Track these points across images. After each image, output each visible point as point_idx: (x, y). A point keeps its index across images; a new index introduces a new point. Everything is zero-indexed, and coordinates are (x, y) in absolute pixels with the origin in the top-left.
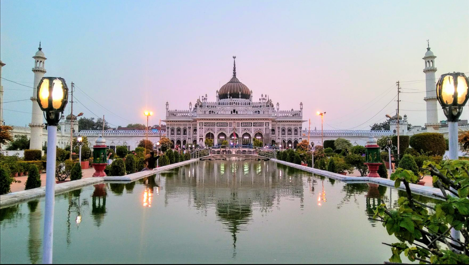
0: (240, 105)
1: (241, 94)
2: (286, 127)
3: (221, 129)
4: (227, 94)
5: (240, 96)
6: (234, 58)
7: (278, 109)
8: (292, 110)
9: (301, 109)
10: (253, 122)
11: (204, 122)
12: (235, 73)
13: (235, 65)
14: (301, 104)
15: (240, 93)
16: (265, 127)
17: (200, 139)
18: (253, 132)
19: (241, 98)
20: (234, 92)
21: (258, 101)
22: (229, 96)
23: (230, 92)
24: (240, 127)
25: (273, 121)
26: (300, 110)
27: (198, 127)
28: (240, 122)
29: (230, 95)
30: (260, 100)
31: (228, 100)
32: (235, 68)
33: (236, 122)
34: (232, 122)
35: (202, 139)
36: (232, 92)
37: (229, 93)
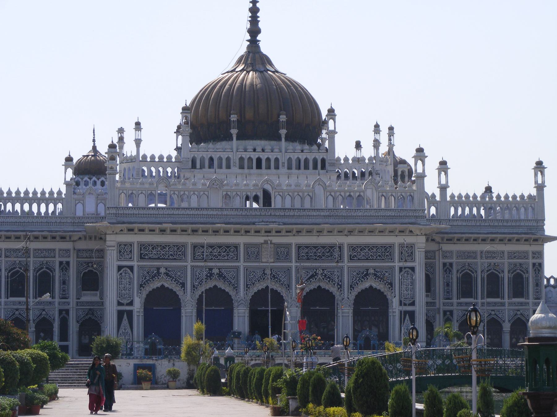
0: (283, 170)
1: (289, 124)
2: (481, 265)
3: (210, 275)
4: (228, 124)
5: (283, 132)
7: (443, 188)
8: (489, 190)
9: (540, 188)
11: (135, 239)
14: (539, 166)
15: (283, 118)
17: (120, 314)
19: (289, 138)
20: (256, 113)
21: (352, 153)
22: (234, 132)
23: (241, 114)
25: (430, 239)
26: (534, 192)
27: (112, 261)
29: (240, 124)
30: (358, 145)
31: (233, 149)
34: (259, 240)
35: (130, 314)
36: (249, 114)
37: (234, 118)
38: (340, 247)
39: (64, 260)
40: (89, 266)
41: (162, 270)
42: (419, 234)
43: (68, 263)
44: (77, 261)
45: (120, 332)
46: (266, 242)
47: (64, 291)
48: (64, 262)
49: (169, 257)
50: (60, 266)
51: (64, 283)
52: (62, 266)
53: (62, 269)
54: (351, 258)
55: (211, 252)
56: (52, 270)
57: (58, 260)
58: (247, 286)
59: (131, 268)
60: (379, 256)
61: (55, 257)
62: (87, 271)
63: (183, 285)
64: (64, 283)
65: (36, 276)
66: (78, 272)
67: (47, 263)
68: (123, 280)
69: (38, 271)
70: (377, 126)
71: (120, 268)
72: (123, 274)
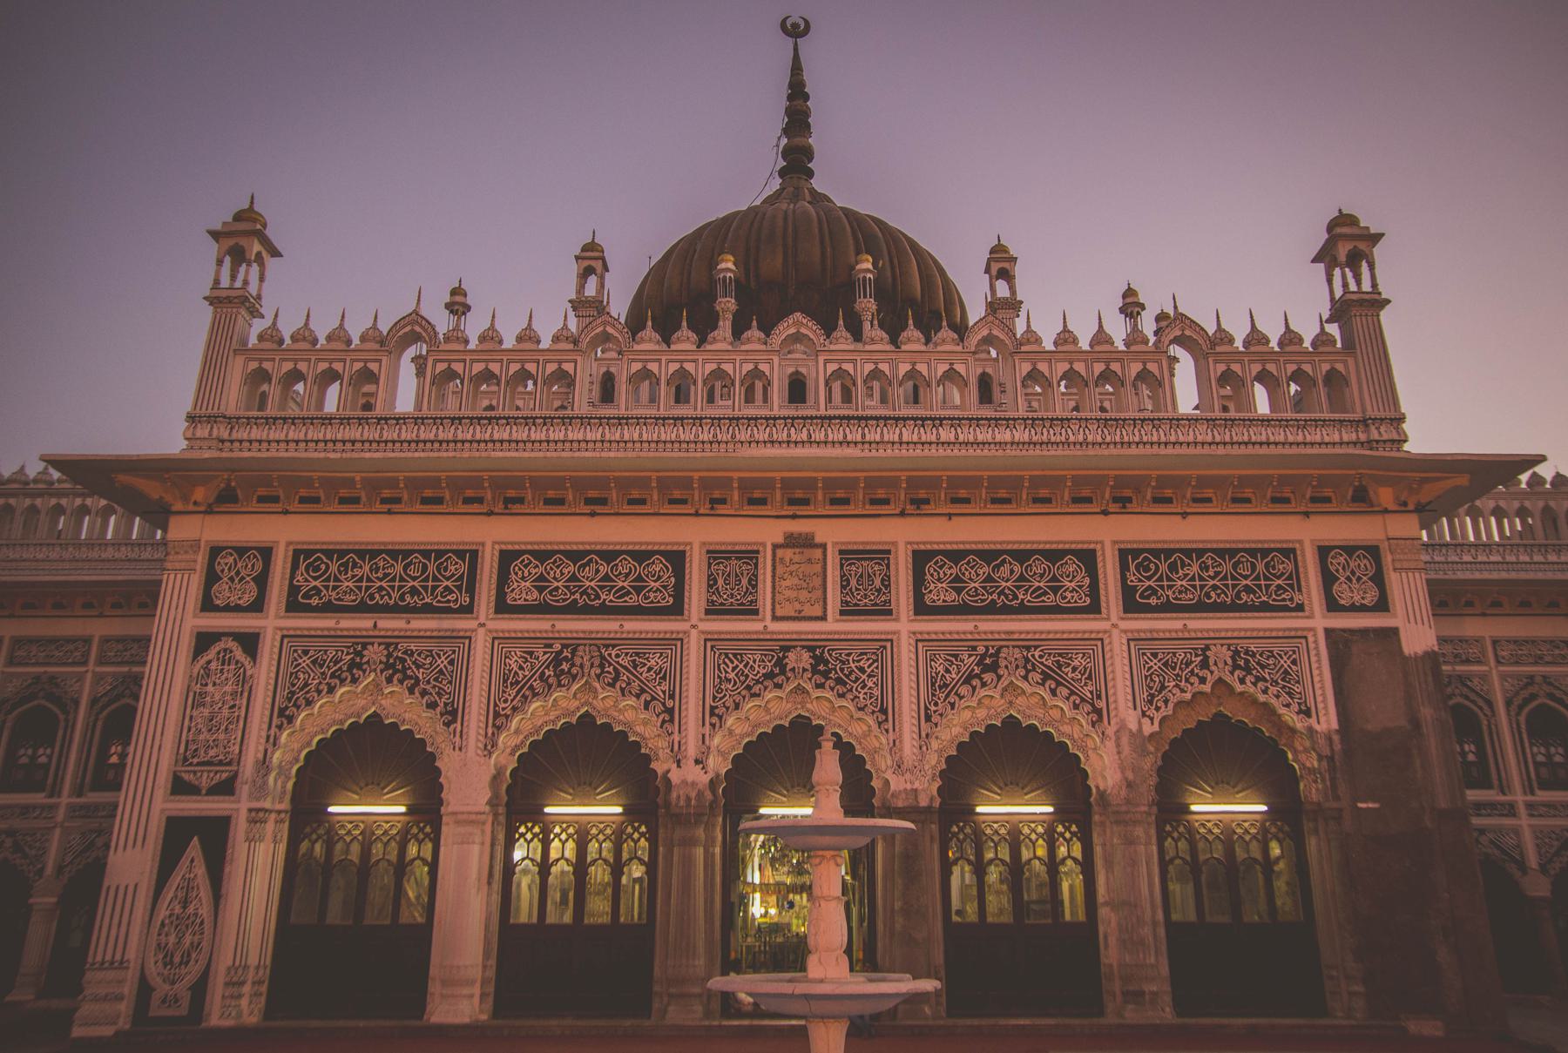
6: (795, 31)
10: (1106, 533)
11: (284, 532)
12: (797, 162)
13: (797, 91)
16: (1319, 621)
17: (178, 832)
18: (1126, 713)
23: (747, 263)
24: (904, 626)
28: (901, 534)
32: (797, 120)
33: (834, 533)
34: (763, 532)
35: (215, 835)
38: (1088, 558)
41: (375, 653)
42: (1391, 507)
45: (163, 913)
46: (792, 541)
49: (402, 598)
54: (1132, 604)
55: (573, 578)
58: (714, 715)
59: (250, 643)
60: (1248, 589)
63: (452, 715)
68: (210, 688)
70: (1129, 293)
71: (204, 641)
72: (213, 666)
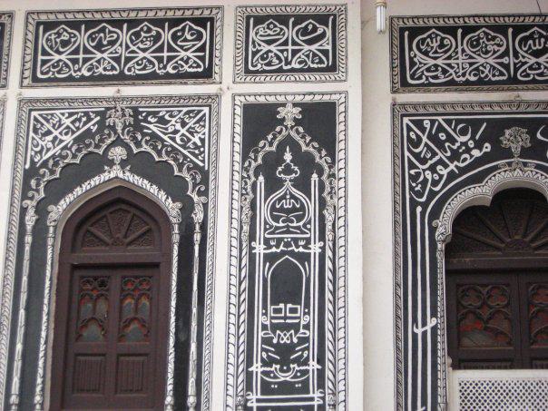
39: (289, 92)
40: (501, 152)
43: (321, 119)
44: (398, 111)
47: (284, 354)
48: (289, 113)
50: (249, 144)
51: (287, 284)
52: (267, 147)
53: (269, 167)
56: (188, 180)
57: (232, 89)
61: (207, 74)
62: (483, 192)
64: (287, 284)
65: (40, 230)
66: (412, 205)
67: (137, 121)
69: (56, 191)
